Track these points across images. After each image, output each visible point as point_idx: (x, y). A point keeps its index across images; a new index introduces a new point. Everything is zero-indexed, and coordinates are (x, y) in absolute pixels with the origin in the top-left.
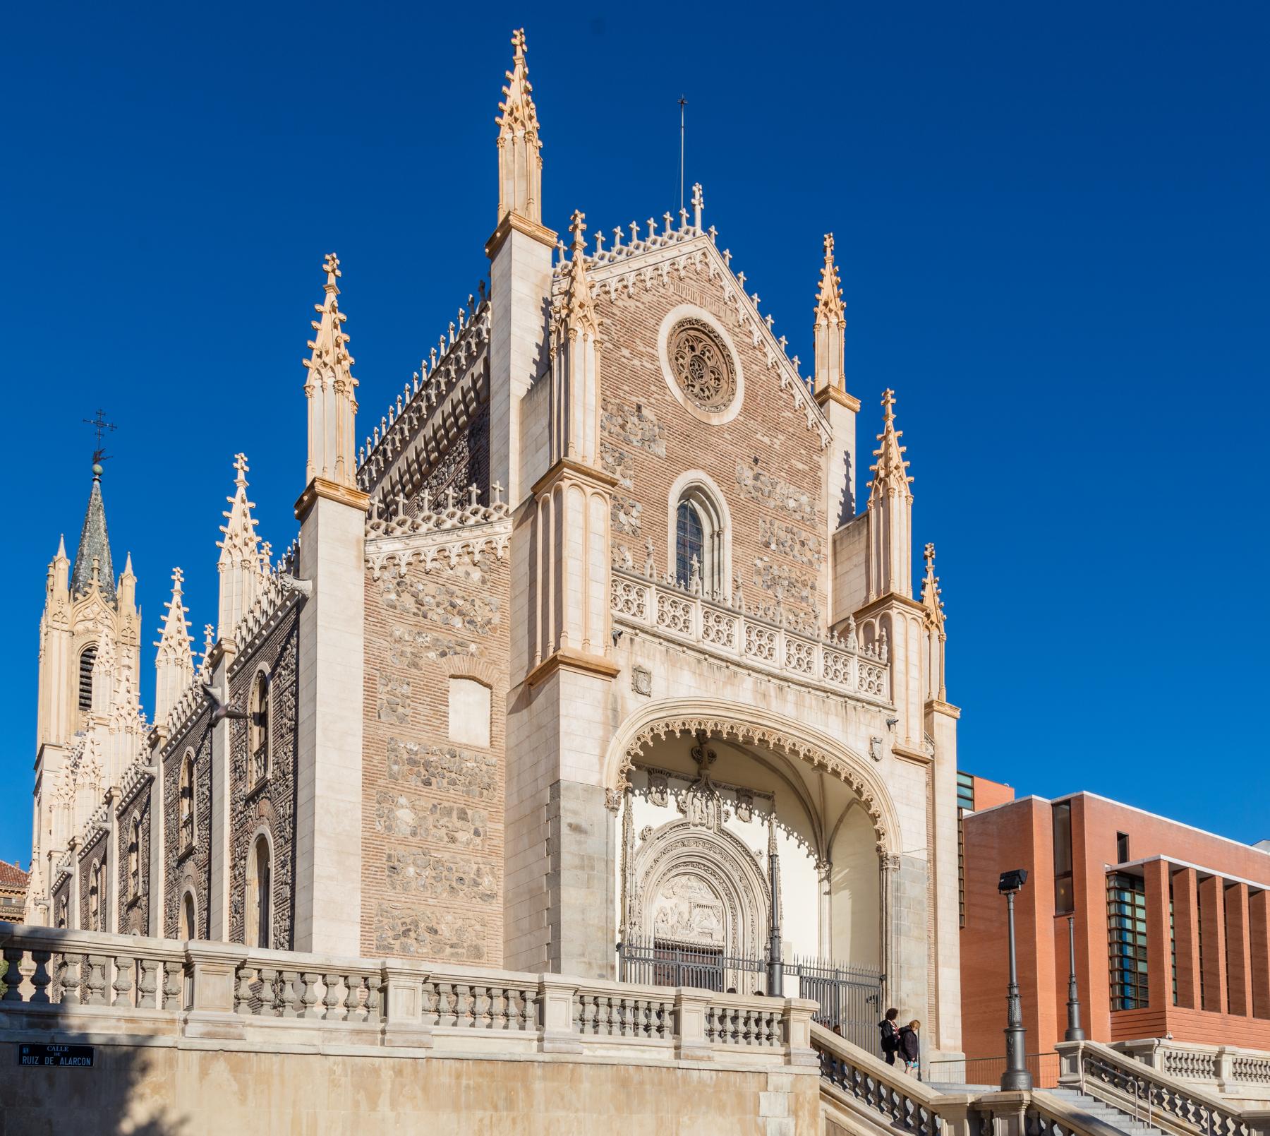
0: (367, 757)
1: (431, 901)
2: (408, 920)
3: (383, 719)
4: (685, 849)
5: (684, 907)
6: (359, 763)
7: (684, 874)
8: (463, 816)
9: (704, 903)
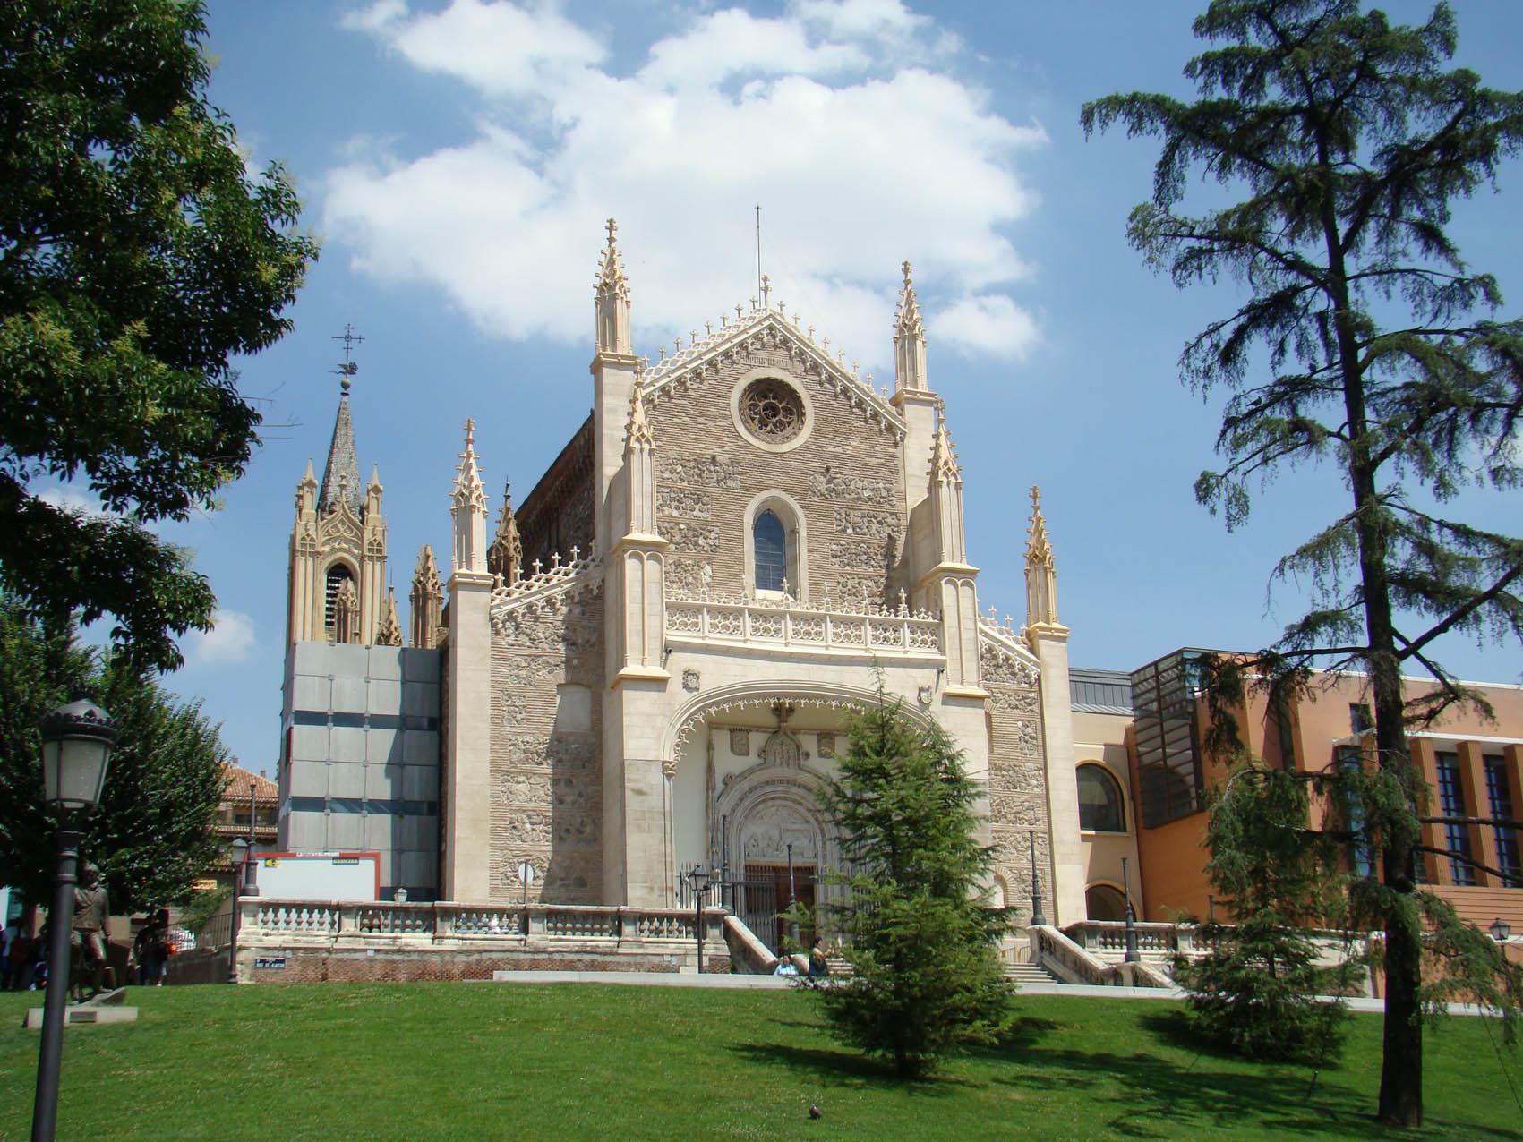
0: (494, 752)
4: (769, 789)
5: (775, 833)
6: (488, 757)
8: (569, 782)
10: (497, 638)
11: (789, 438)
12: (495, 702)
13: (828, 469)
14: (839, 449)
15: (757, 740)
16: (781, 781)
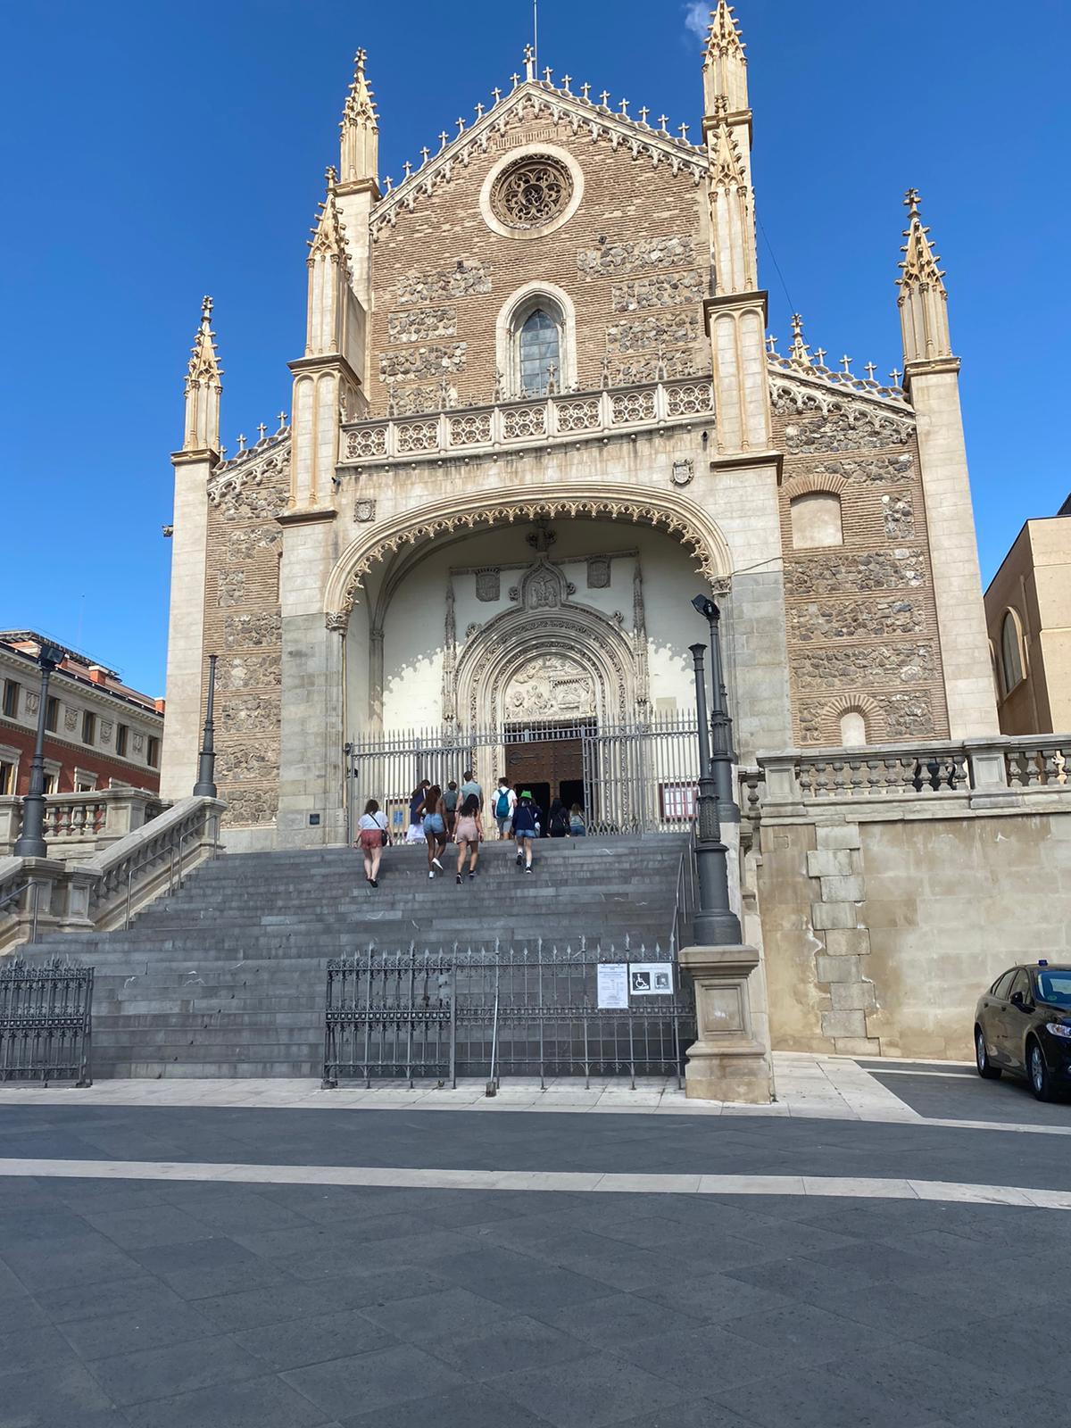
1: (259, 735)
2: (239, 755)
3: (222, 604)
4: (527, 635)
5: (545, 688)
7: (540, 655)
9: (566, 678)
10: (217, 515)
11: (552, 218)
12: (211, 583)
13: (602, 241)
14: (618, 214)
15: (509, 580)
16: (544, 623)
